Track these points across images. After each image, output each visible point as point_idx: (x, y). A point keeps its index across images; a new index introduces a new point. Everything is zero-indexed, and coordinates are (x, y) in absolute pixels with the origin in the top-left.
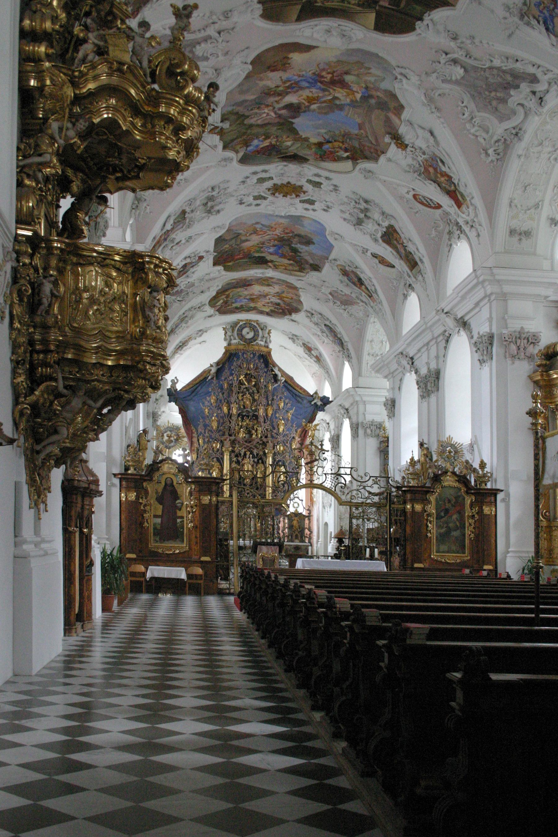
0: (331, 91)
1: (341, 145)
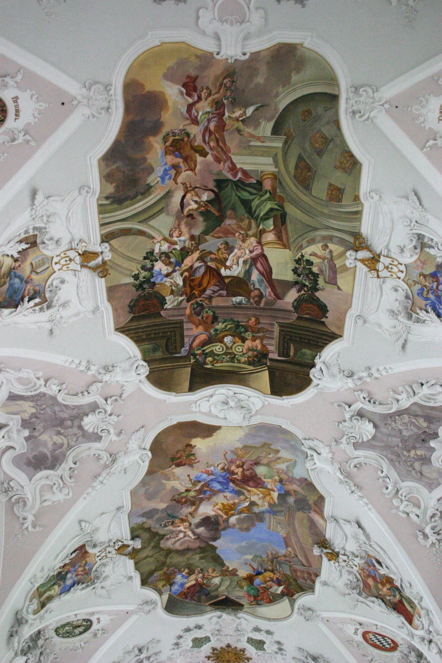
0: (245, 492)
1: (272, 575)
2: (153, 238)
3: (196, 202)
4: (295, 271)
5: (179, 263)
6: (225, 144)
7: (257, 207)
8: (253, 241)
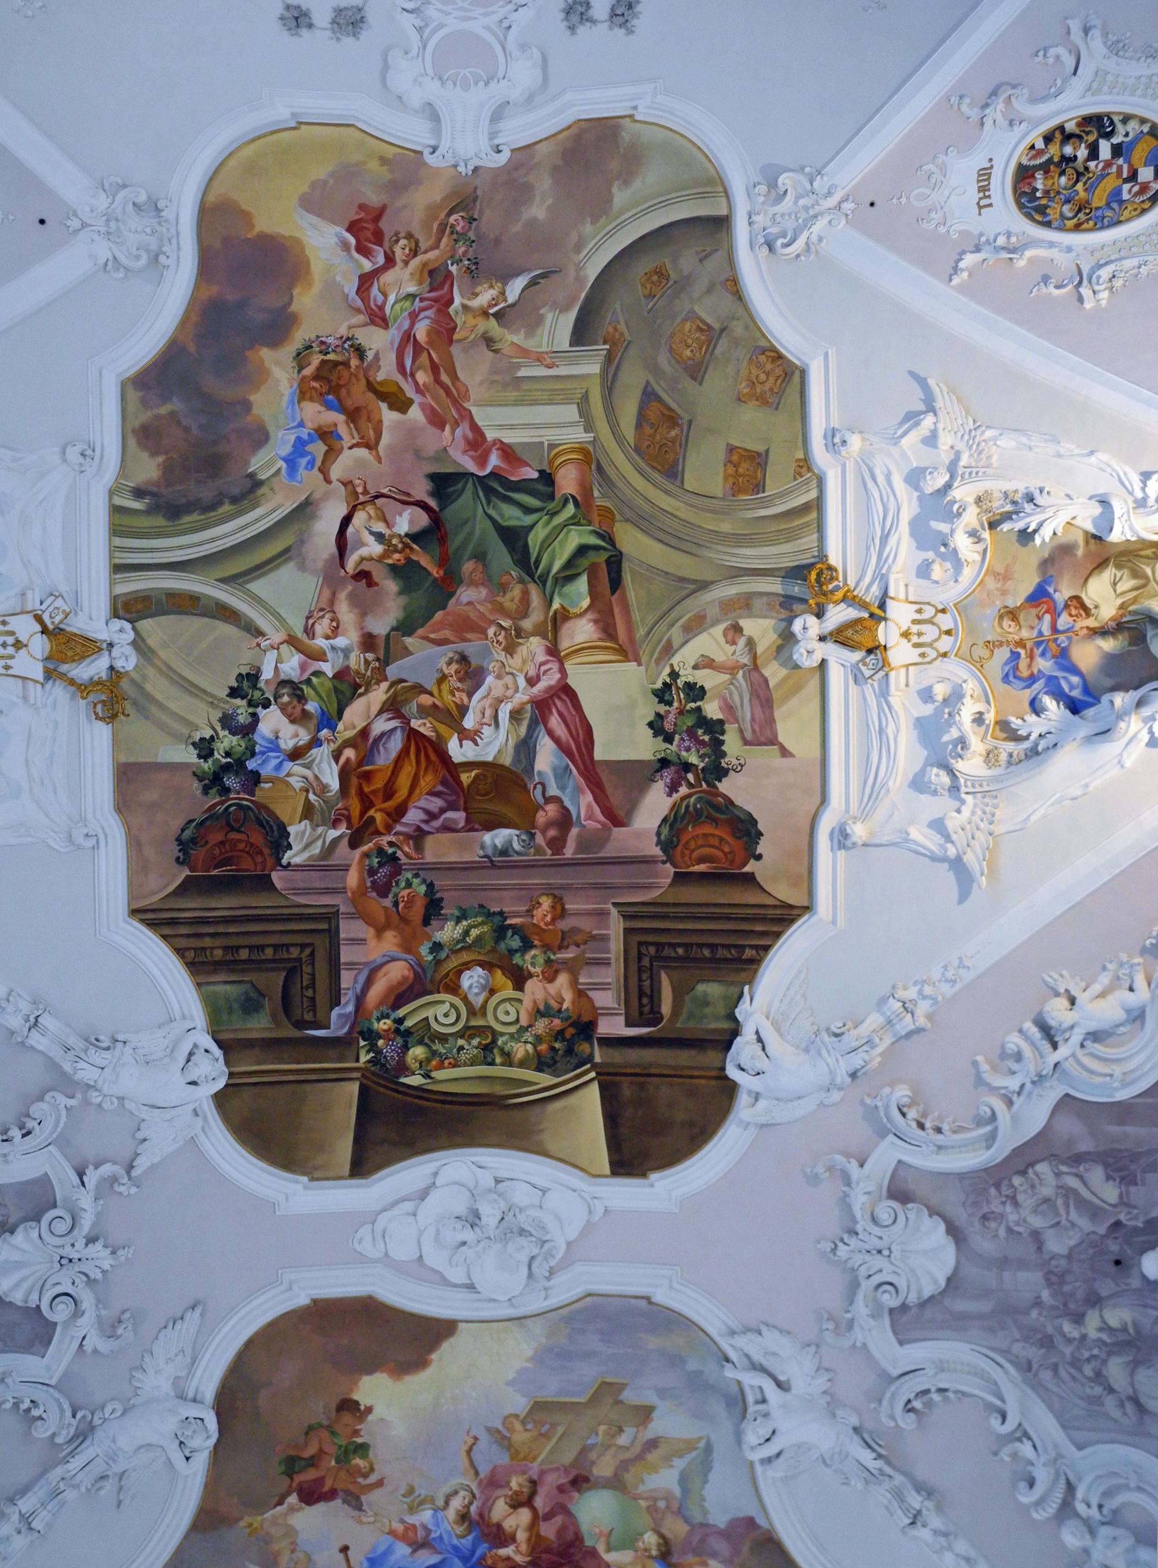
2: (260, 633)
3: (379, 537)
4: (657, 726)
5: (329, 720)
6: (454, 377)
7: (546, 543)
8: (535, 646)
